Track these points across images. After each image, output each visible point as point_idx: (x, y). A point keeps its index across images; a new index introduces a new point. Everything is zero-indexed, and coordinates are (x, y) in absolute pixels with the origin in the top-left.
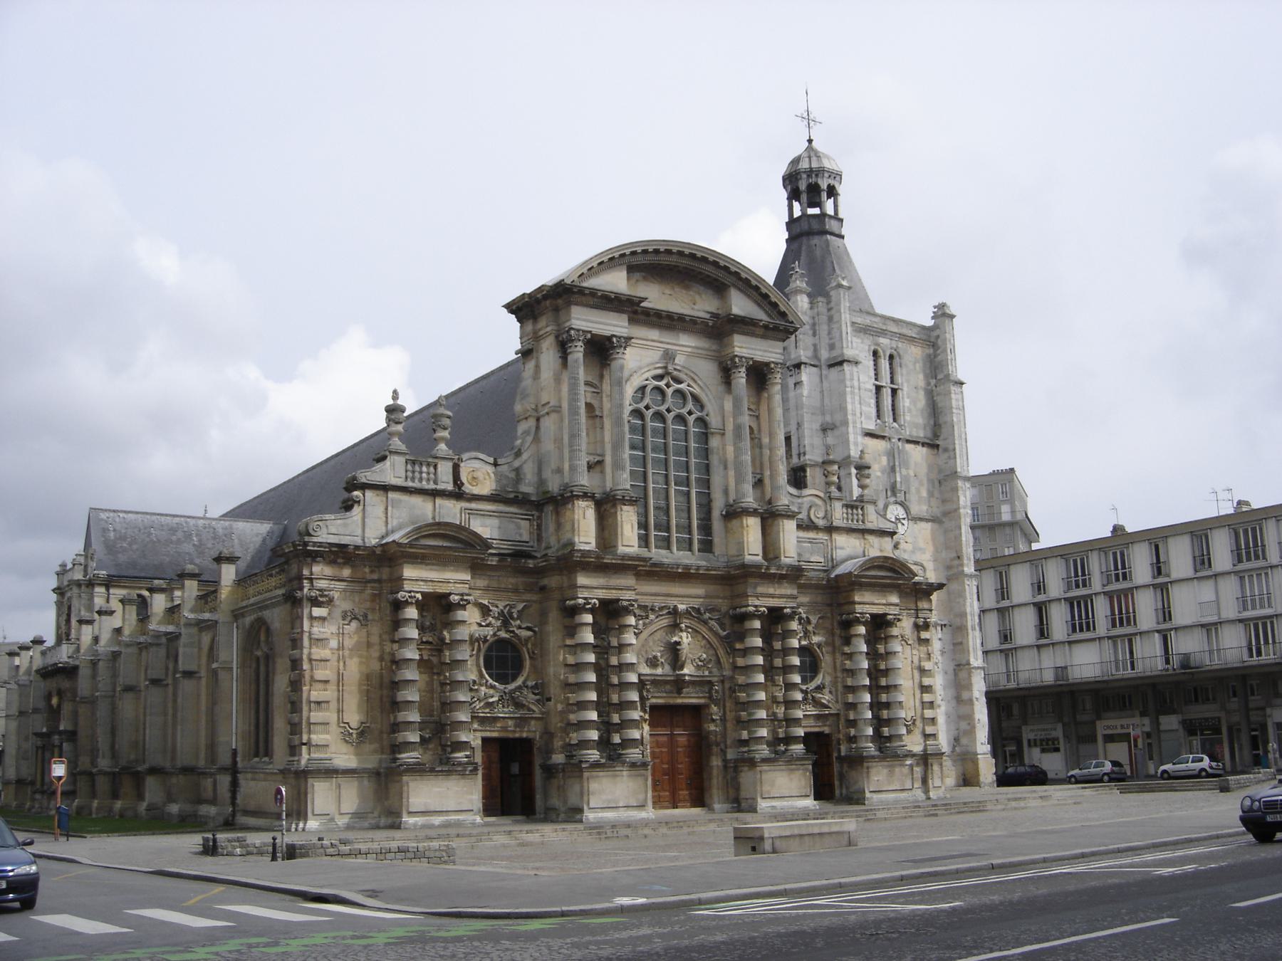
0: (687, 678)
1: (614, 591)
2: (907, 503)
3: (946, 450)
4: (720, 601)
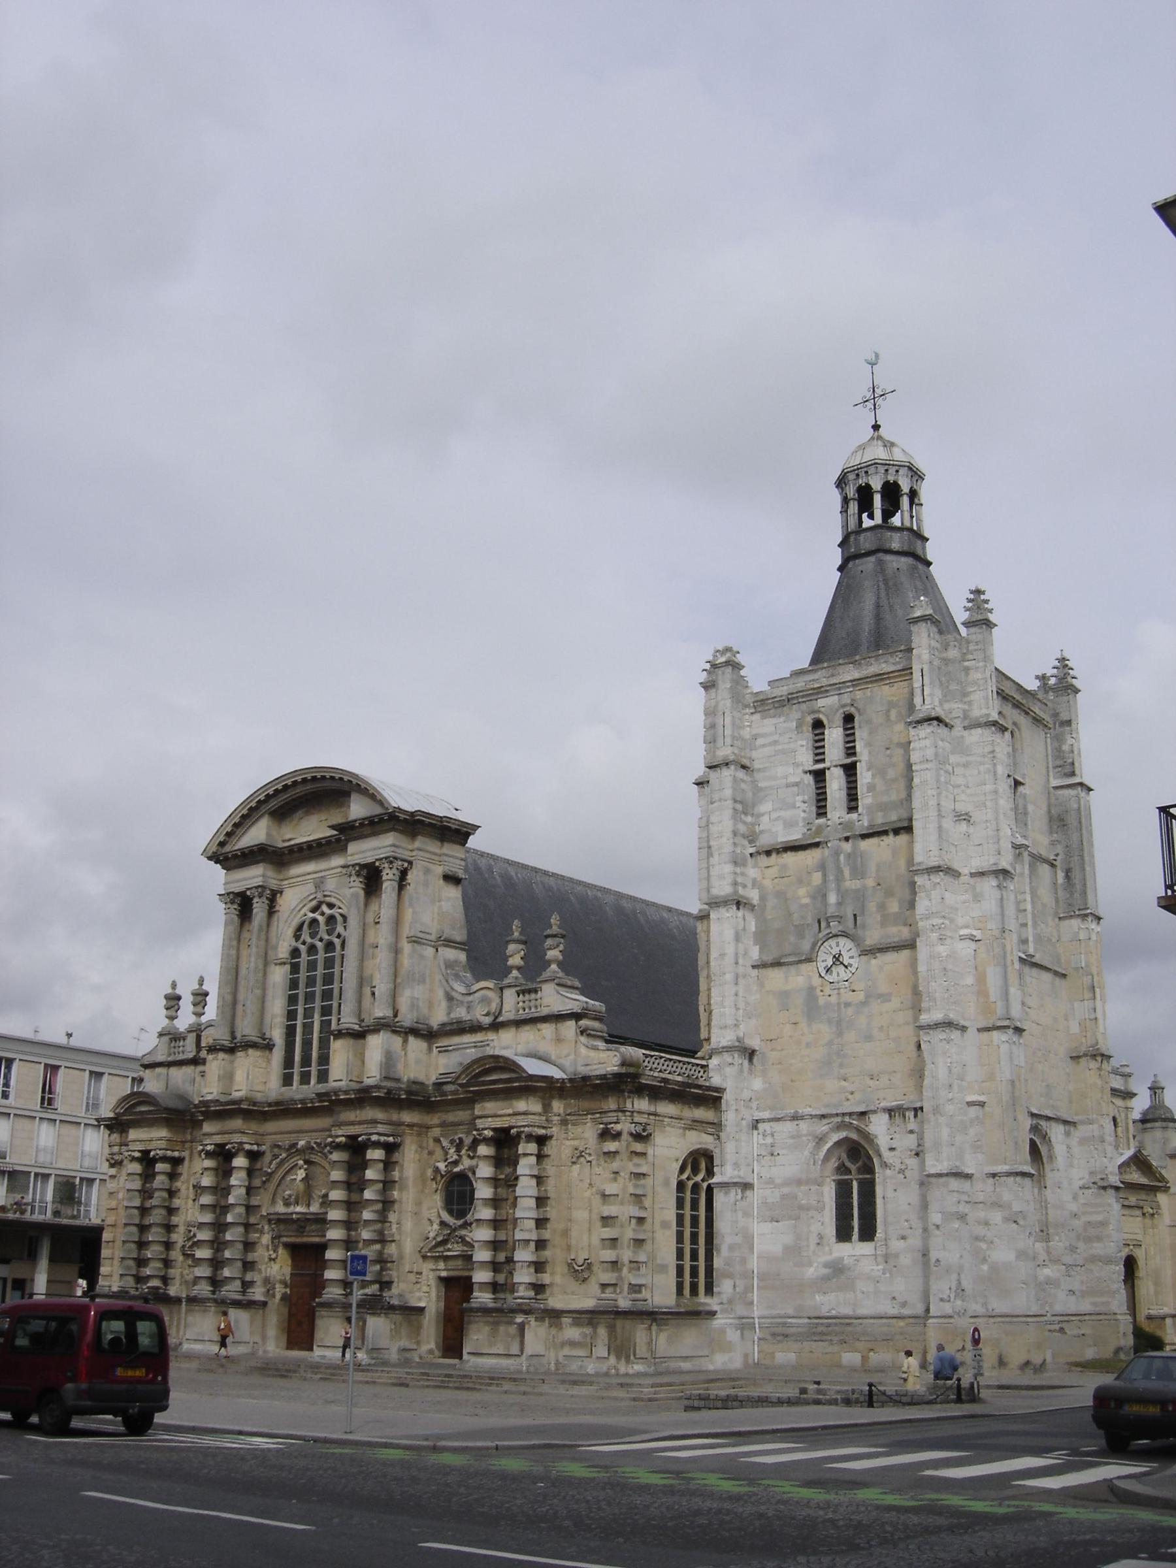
0: (294, 1216)
2: (860, 932)
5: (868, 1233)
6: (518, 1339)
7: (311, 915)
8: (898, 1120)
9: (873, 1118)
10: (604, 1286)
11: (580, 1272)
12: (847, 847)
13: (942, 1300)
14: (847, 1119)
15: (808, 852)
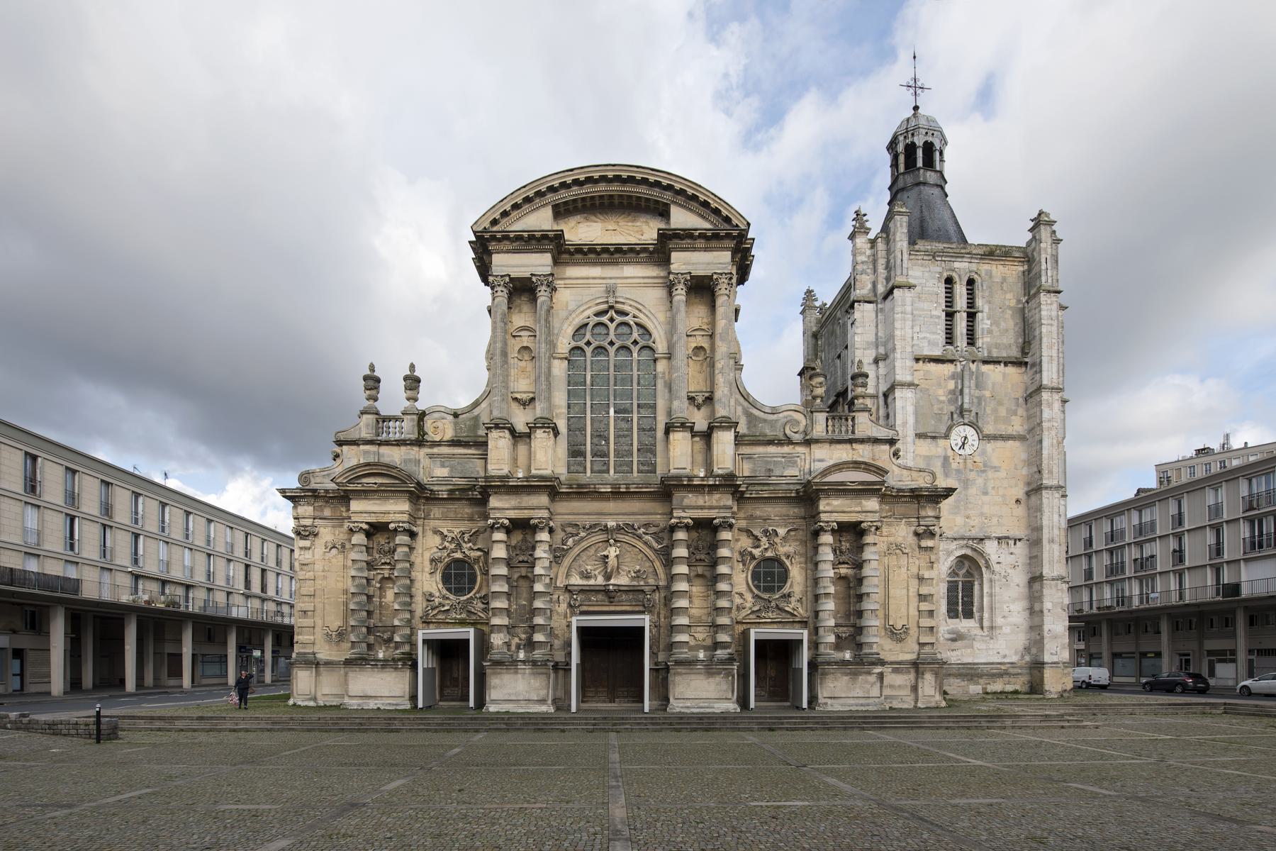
0: (611, 587)
1: (526, 511)
3: (1033, 365)
4: (659, 516)
5: (969, 614)
6: (878, 685)
7: (597, 319)
8: (1004, 546)
9: (987, 542)
10: (921, 645)
11: (896, 635)
12: (973, 367)
13: (1051, 654)
14: (971, 543)
15: (945, 365)
